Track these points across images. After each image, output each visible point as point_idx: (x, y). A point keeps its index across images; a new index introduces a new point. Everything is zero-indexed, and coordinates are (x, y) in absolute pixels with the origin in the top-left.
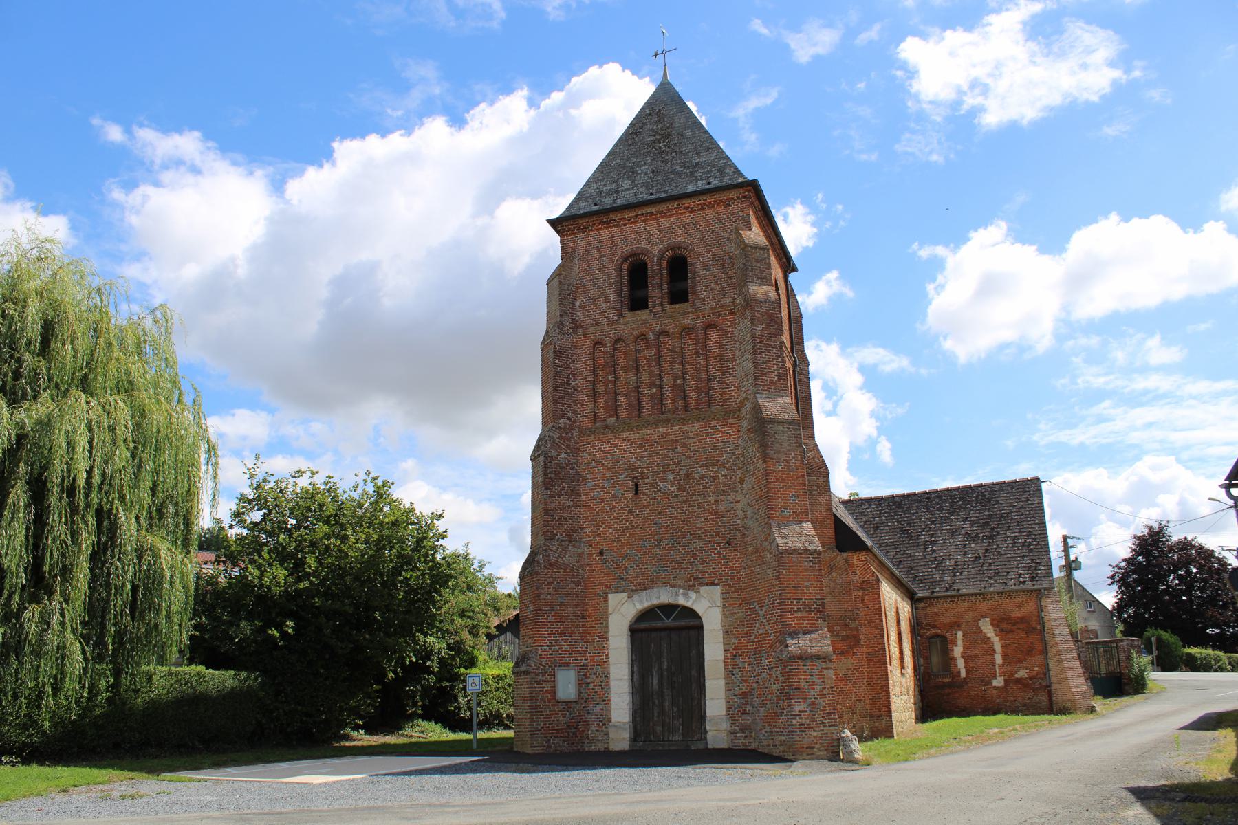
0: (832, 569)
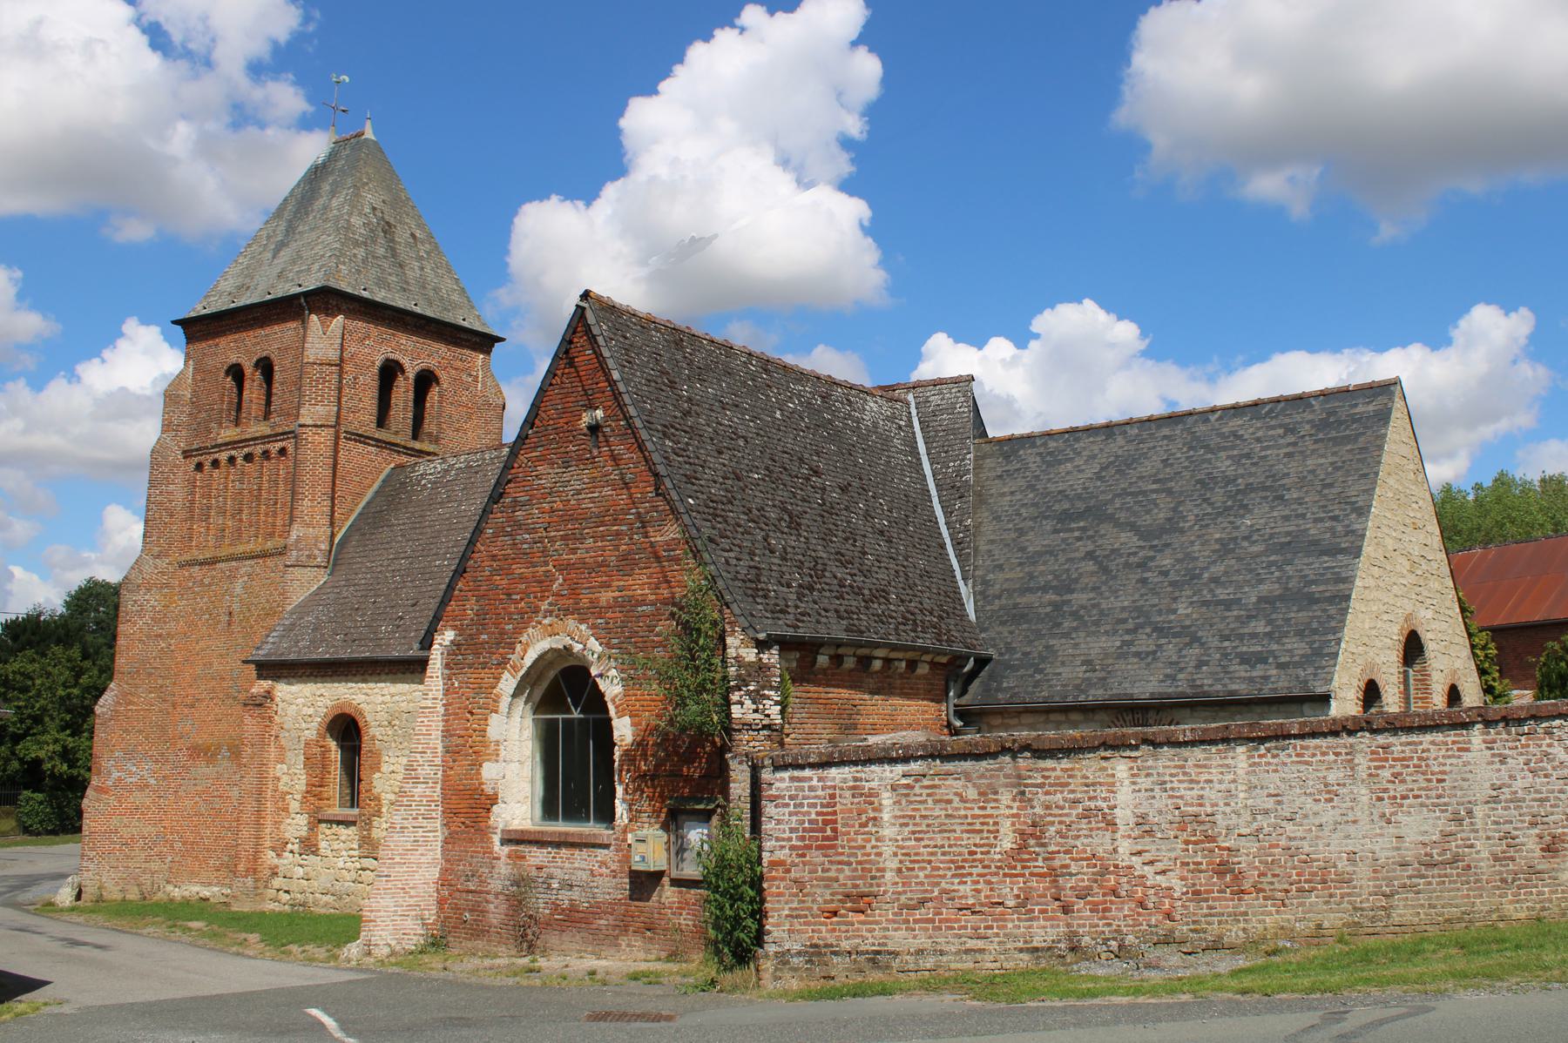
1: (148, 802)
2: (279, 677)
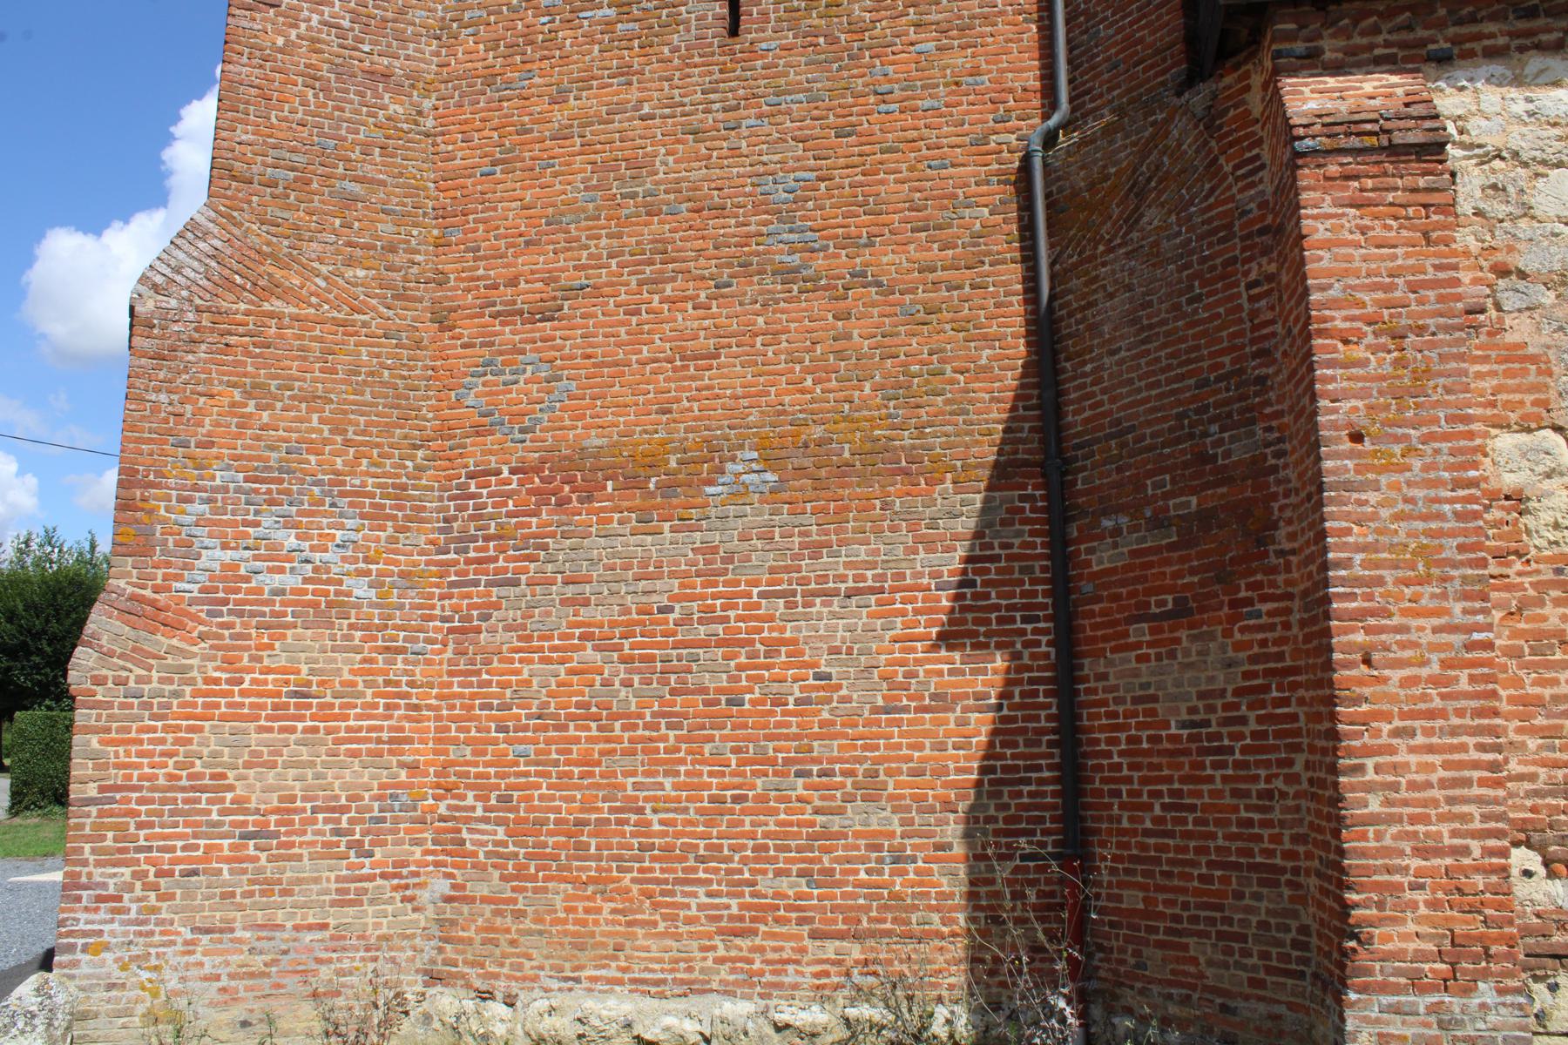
0: (1141, 196)
1: (345, 666)
2: (1443, 60)
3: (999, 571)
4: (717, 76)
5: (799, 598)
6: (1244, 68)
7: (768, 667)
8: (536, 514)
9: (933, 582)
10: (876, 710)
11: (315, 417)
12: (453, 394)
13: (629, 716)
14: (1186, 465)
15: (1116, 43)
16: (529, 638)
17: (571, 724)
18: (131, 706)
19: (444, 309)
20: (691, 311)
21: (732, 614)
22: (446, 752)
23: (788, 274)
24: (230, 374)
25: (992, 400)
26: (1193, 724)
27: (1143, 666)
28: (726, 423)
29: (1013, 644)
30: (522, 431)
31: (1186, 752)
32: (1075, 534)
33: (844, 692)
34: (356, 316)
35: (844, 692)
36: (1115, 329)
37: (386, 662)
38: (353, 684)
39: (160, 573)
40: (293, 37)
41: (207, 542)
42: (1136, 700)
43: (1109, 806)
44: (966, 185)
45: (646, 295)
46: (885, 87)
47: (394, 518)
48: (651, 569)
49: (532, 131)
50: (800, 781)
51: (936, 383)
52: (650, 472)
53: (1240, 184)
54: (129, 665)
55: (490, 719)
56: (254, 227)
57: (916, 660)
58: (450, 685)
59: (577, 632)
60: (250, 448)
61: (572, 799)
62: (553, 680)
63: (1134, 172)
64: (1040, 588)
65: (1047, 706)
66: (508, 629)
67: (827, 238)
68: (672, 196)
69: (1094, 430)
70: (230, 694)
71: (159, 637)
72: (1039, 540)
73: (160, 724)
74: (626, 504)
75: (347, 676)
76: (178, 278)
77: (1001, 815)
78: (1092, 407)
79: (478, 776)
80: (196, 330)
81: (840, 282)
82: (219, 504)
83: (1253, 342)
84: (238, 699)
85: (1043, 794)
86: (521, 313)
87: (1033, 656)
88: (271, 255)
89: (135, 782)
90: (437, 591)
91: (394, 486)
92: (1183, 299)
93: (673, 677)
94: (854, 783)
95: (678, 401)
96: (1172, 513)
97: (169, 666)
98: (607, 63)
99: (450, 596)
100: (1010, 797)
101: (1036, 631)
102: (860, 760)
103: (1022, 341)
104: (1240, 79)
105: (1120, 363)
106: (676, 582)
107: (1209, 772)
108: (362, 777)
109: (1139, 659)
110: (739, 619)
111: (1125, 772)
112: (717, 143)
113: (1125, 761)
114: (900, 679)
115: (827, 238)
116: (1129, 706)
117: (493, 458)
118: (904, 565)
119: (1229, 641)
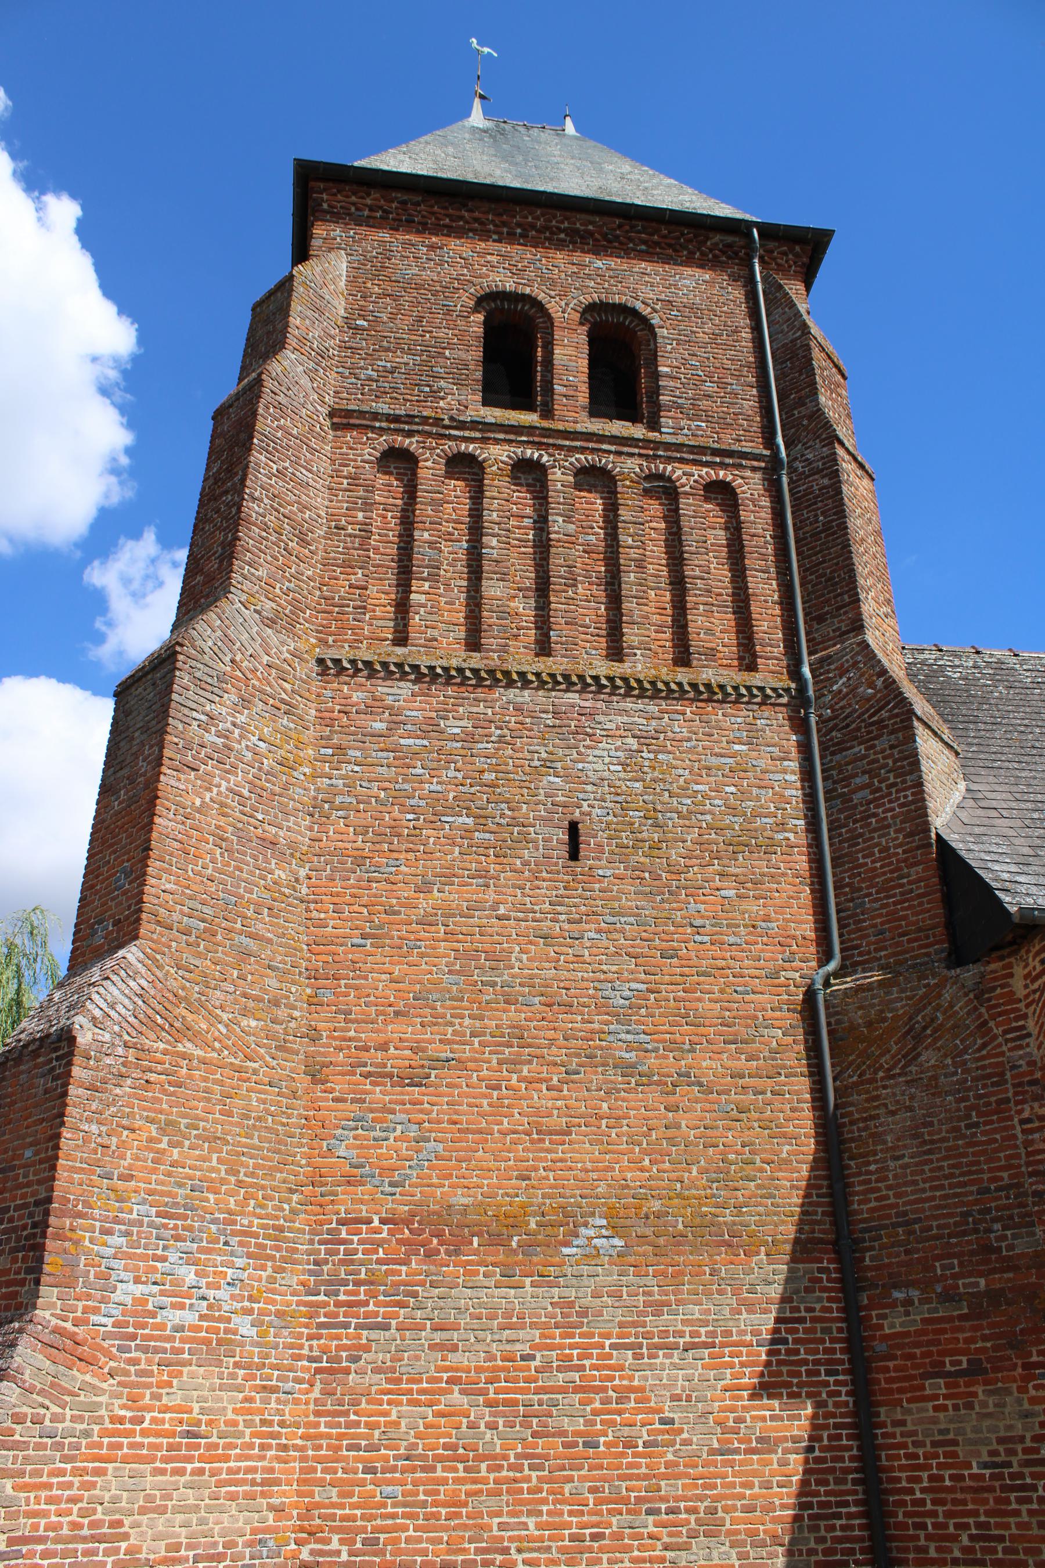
0: (919, 1039)
1: (229, 1403)
3: (806, 1331)
4: (561, 892)
5: (645, 1350)
6: (1007, 961)
7: (620, 1413)
8: (406, 1262)
9: (754, 1339)
10: (712, 1452)
11: (215, 1156)
12: (325, 1143)
13: (494, 1457)
14: (972, 1253)
15: (881, 915)
16: (398, 1381)
17: (439, 1465)
18: (44, 1447)
19: (318, 1063)
20: (545, 1091)
21: (587, 1363)
22: (311, 1494)
23: (627, 1069)
24: (149, 1110)
25: (792, 1187)
26: (995, 1465)
27: (941, 1415)
28: (578, 1192)
29: (820, 1394)
30: (391, 1184)
31: (991, 1489)
32: (866, 1302)
33: (685, 1435)
34: (249, 1064)
35: (685, 1435)
36: (898, 1139)
37: (262, 1401)
38: (235, 1423)
39: (80, 1304)
40: (207, 800)
41: (124, 1275)
42: (934, 1444)
43: (917, 1538)
44: (764, 1010)
45: (505, 1073)
46: (698, 922)
47: (272, 1258)
48: (515, 1319)
49: (399, 913)
50: (651, 1518)
51: (749, 1170)
52: (512, 1231)
53: (1009, 1045)
54: (47, 1402)
55: (357, 1459)
56: (172, 971)
57: (743, 1407)
58: (317, 1425)
59: (445, 1376)
60: (162, 1183)
61: (438, 1541)
62: (421, 1421)
63: (911, 1019)
64: (837, 1346)
65: (849, 1448)
66: (376, 1371)
67: (658, 1041)
68: (527, 989)
69: (880, 1218)
70: (129, 1434)
71: (75, 1372)
72: (834, 1306)
73: (69, 1466)
74: (490, 1259)
75: (230, 1416)
76: (112, 1013)
77: (820, 1547)
78: (876, 1199)
79: (344, 1518)
80: (124, 1064)
81: (669, 1079)
82: (135, 1238)
83: (1028, 1164)
84: (138, 1439)
85: (851, 1528)
86: (391, 1076)
87: (836, 1405)
88: (185, 999)
89: (41, 1532)
90: (306, 1331)
91: (275, 1228)
92: (963, 1124)
93: (535, 1421)
94: (696, 1520)
95: (536, 1169)
96: (962, 1290)
97: (81, 1402)
98: (467, 865)
99: (319, 1337)
100: (826, 1531)
101: (837, 1383)
102: (701, 1498)
103: (812, 1140)
104: (1004, 968)
105: (904, 1167)
106: (537, 1333)
107: (1014, 1506)
108: (237, 1521)
109: (936, 1408)
110: (594, 1367)
111: (929, 1506)
112: (564, 949)
113: (928, 1497)
114: (731, 1424)
115: (658, 1041)
116: (928, 1448)
117: (364, 1208)
118: (731, 1323)
119: (1025, 1396)
